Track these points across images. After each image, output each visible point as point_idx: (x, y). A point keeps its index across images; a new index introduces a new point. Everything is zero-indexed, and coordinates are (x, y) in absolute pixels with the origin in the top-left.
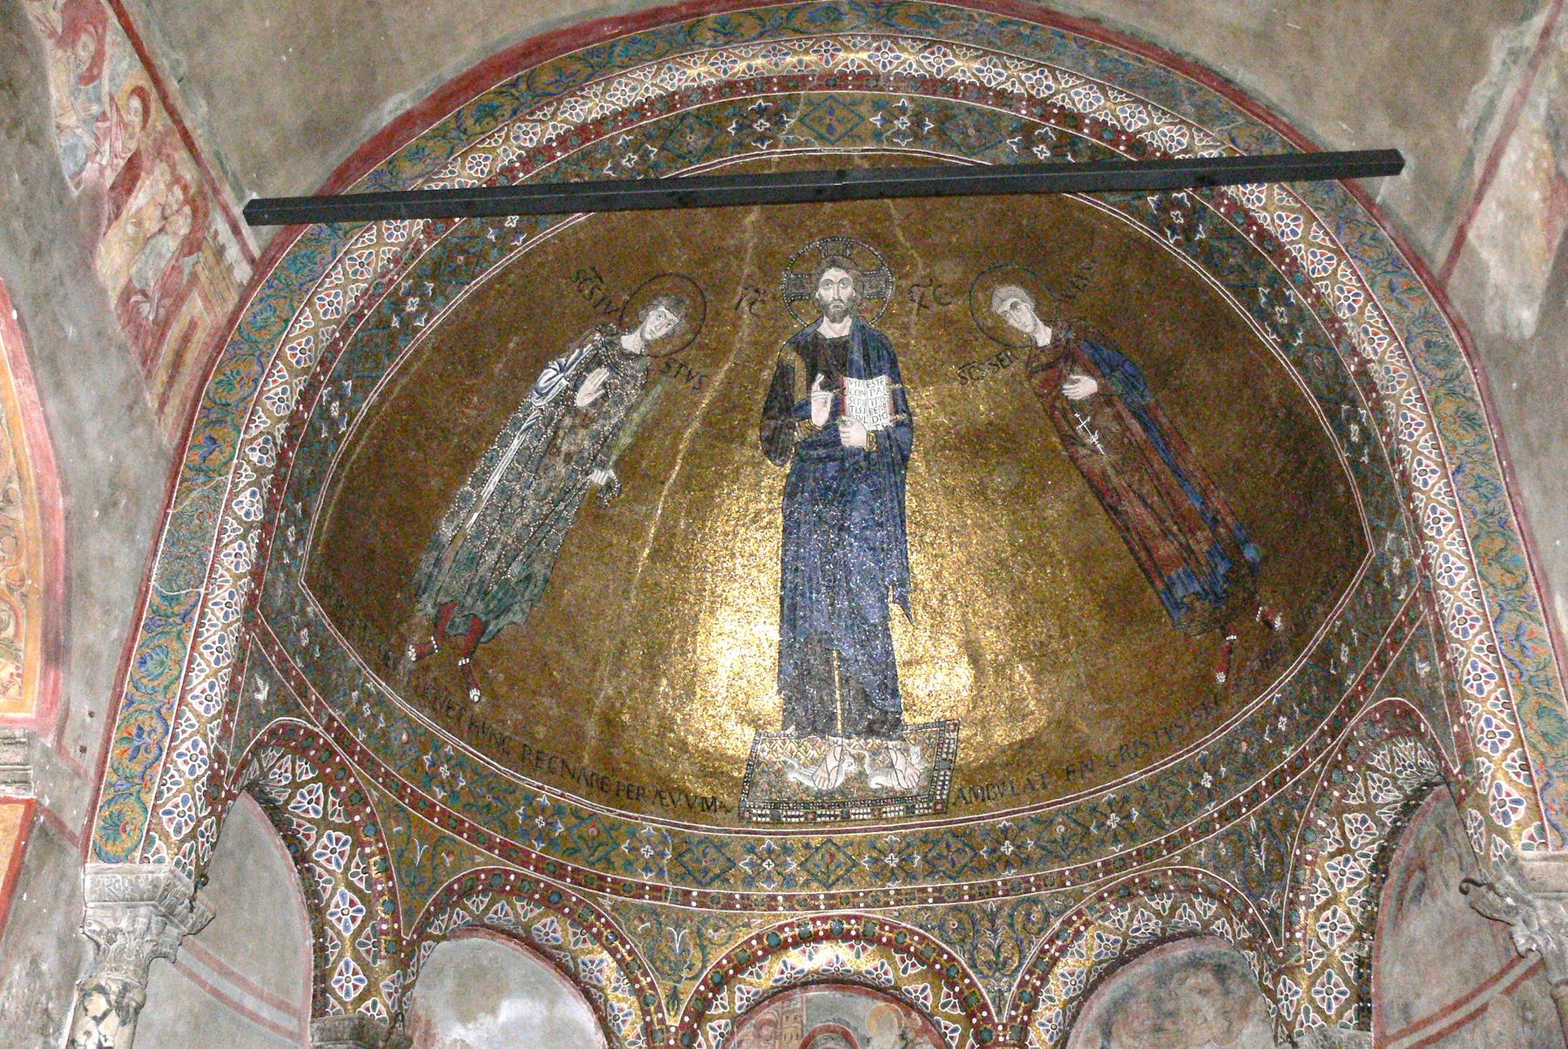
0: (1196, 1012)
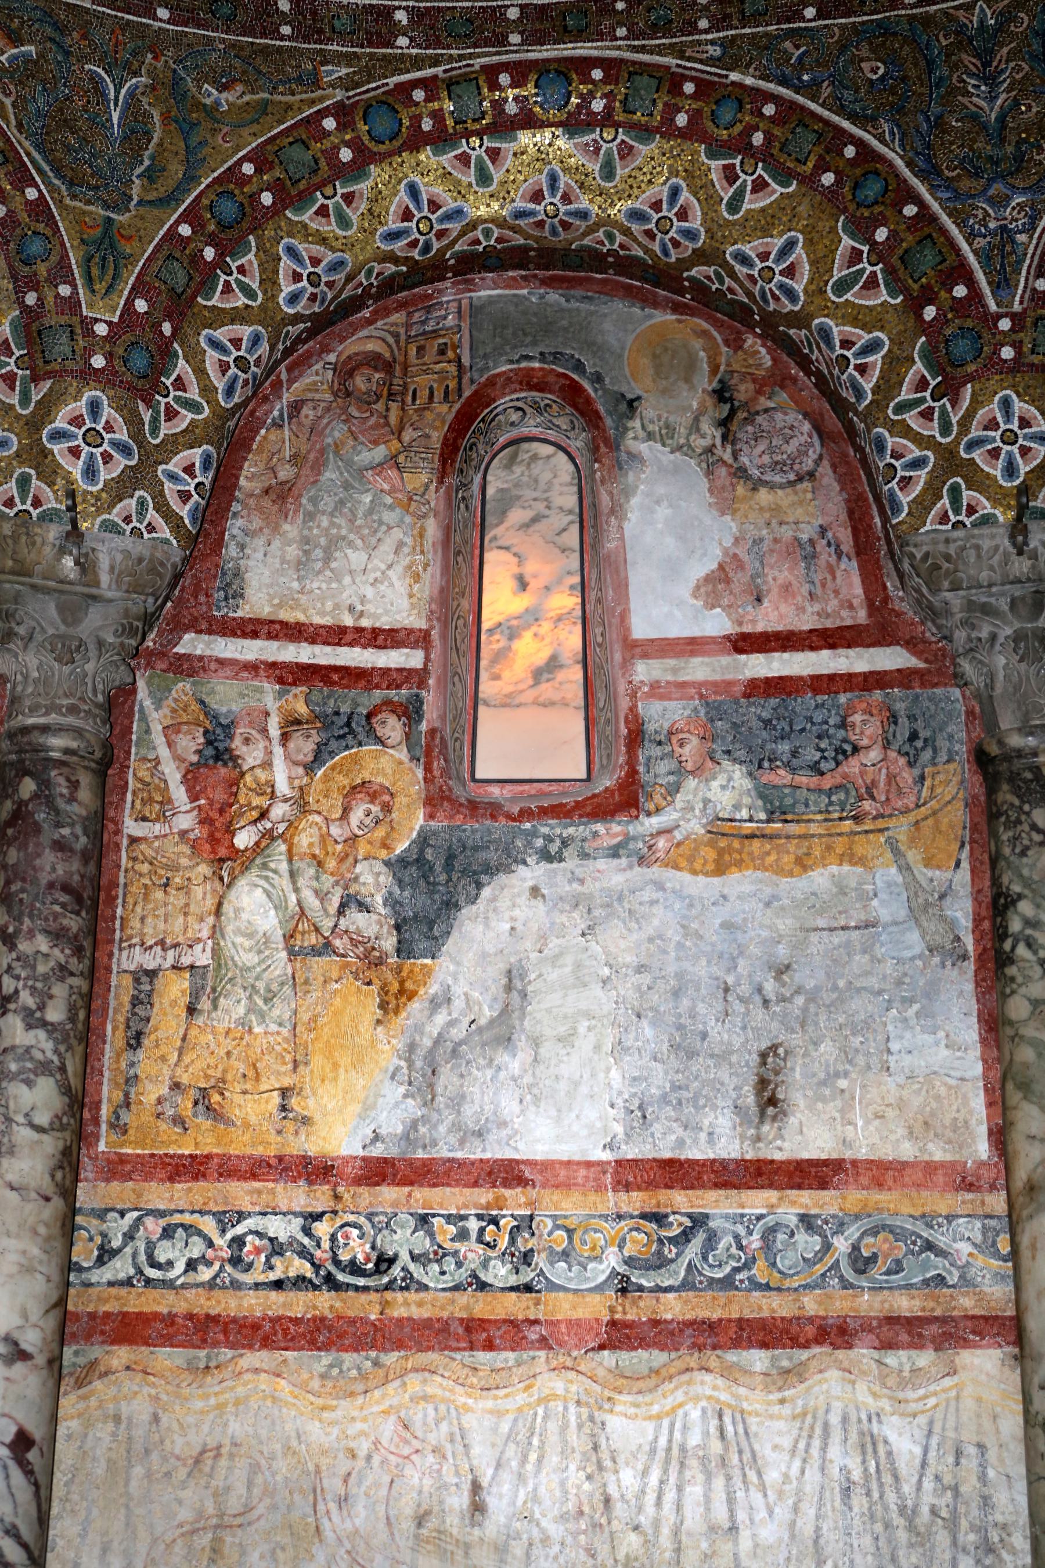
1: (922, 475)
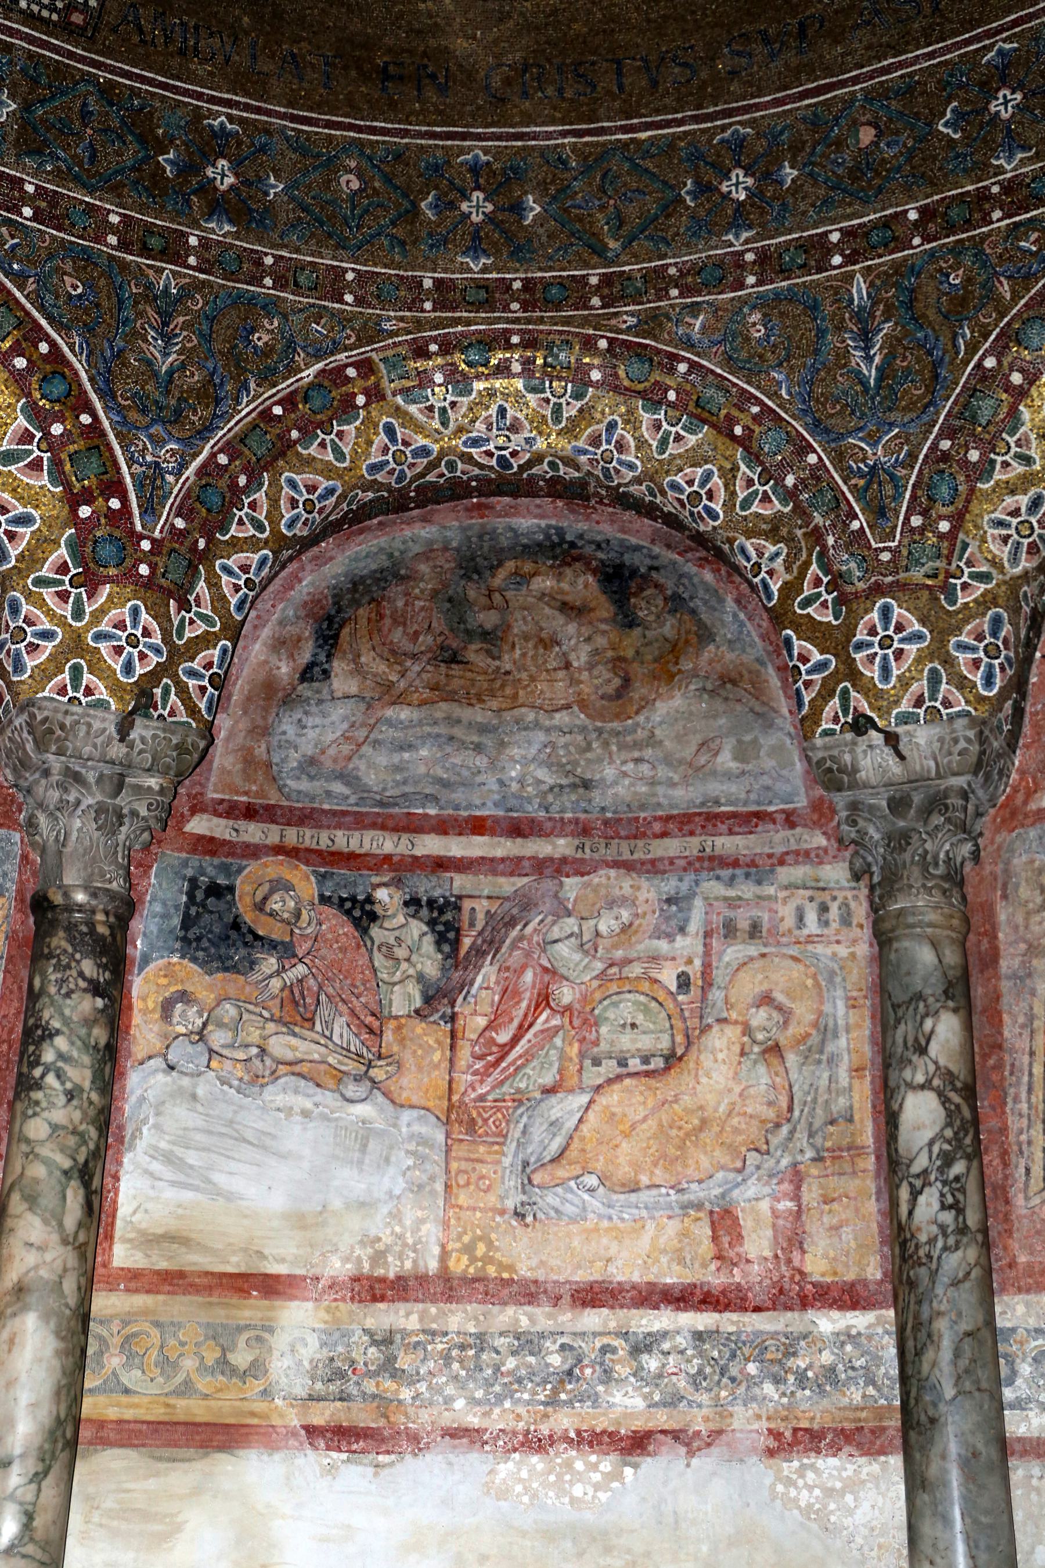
0: (549, 643)
1: (49, 647)
